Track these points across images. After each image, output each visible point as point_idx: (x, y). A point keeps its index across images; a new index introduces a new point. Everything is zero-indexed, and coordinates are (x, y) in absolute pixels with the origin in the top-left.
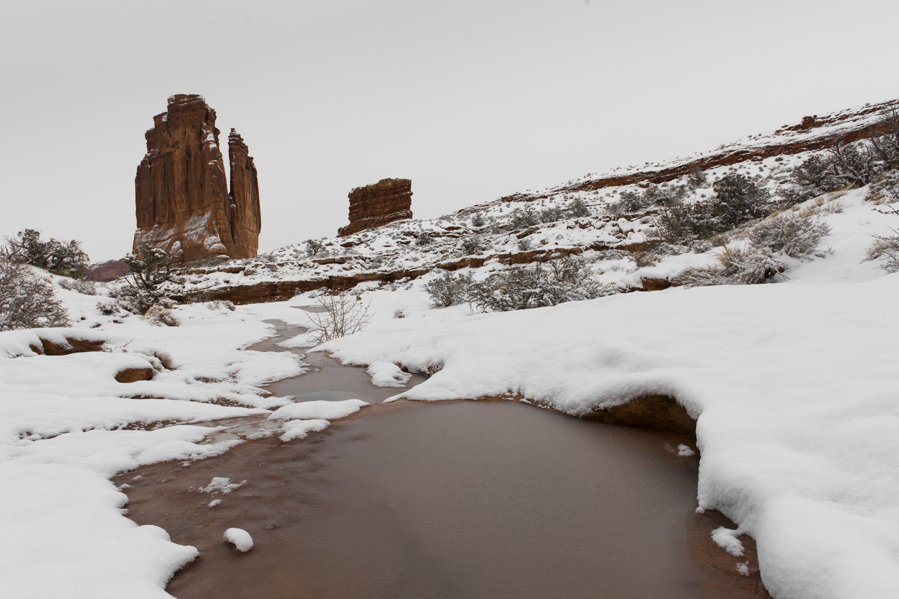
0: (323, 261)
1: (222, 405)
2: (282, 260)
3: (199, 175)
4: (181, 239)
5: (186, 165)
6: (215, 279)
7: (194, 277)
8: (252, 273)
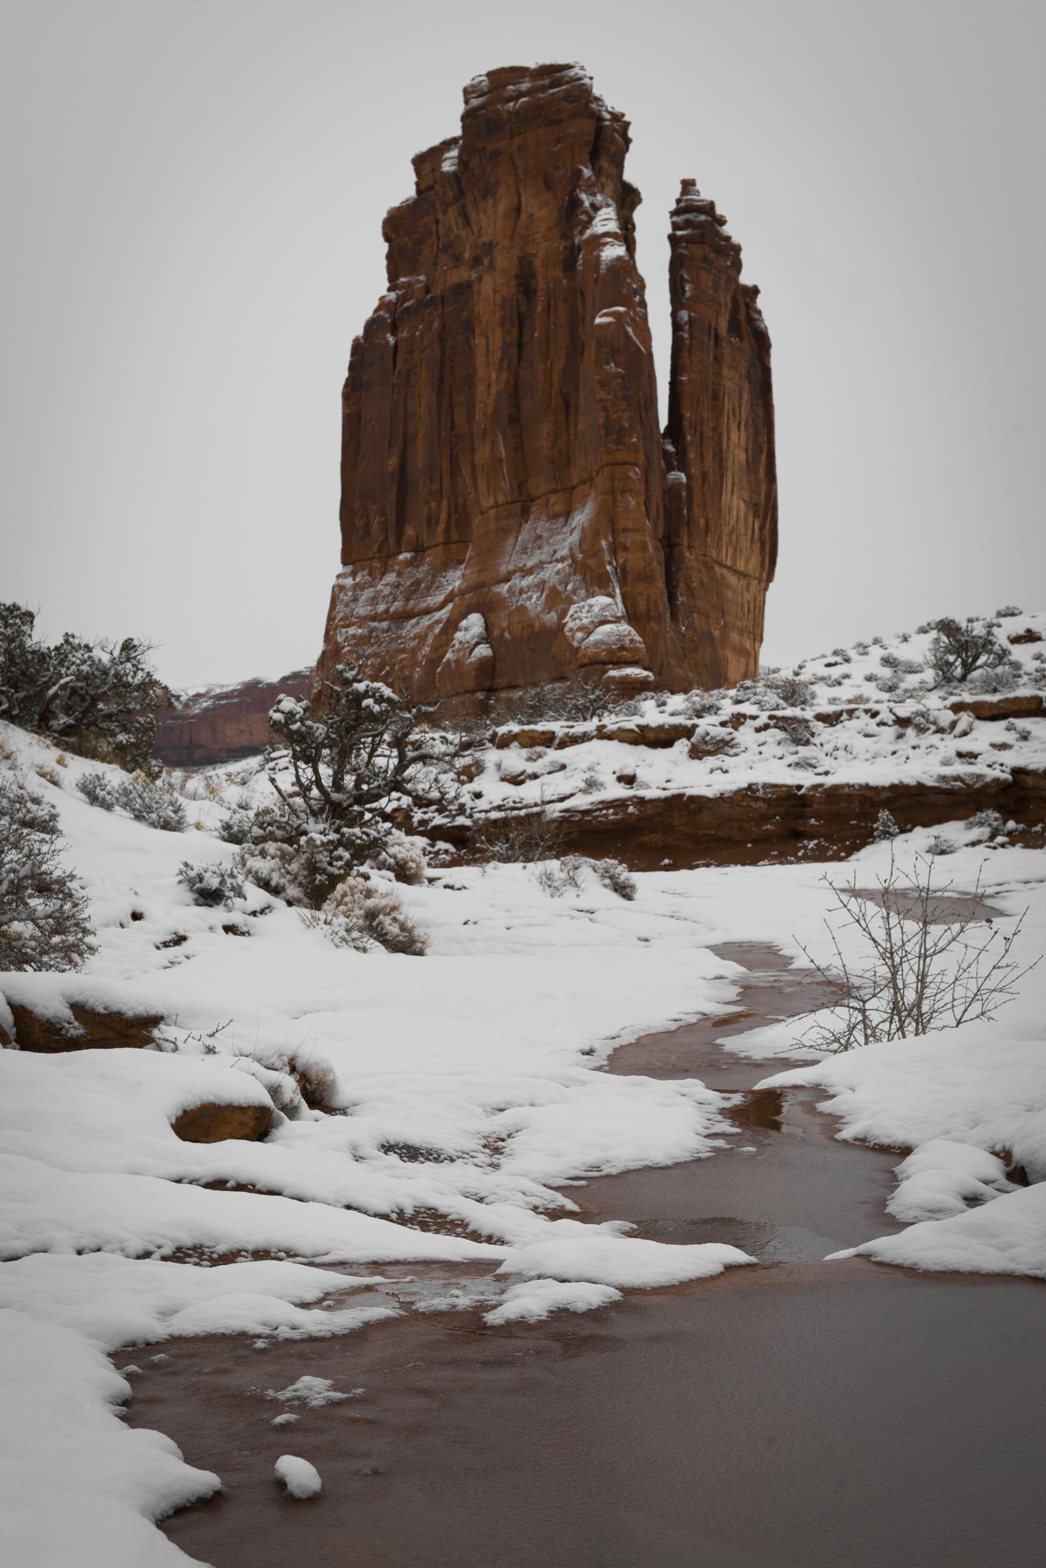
0: (991, 705)
1: (423, 1230)
2: (833, 701)
3: (559, 365)
4: (487, 607)
5: (515, 333)
6: (584, 766)
7: (515, 759)
8: (721, 747)
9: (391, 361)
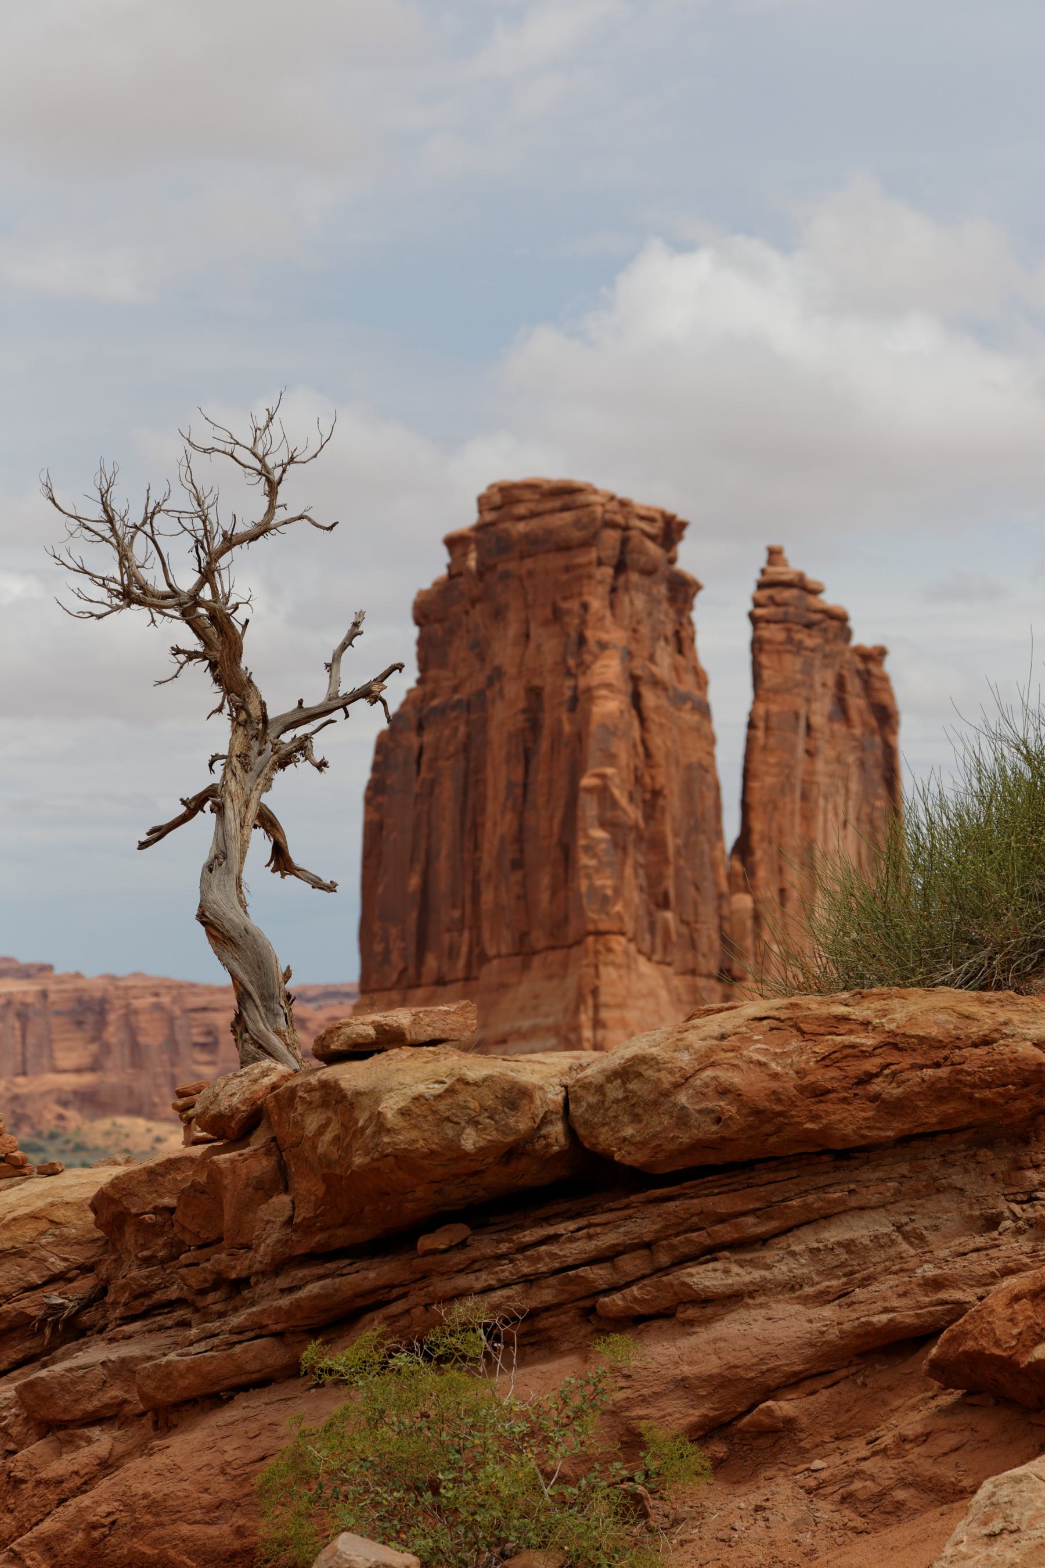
5: (520, 771)
9: (414, 766)
